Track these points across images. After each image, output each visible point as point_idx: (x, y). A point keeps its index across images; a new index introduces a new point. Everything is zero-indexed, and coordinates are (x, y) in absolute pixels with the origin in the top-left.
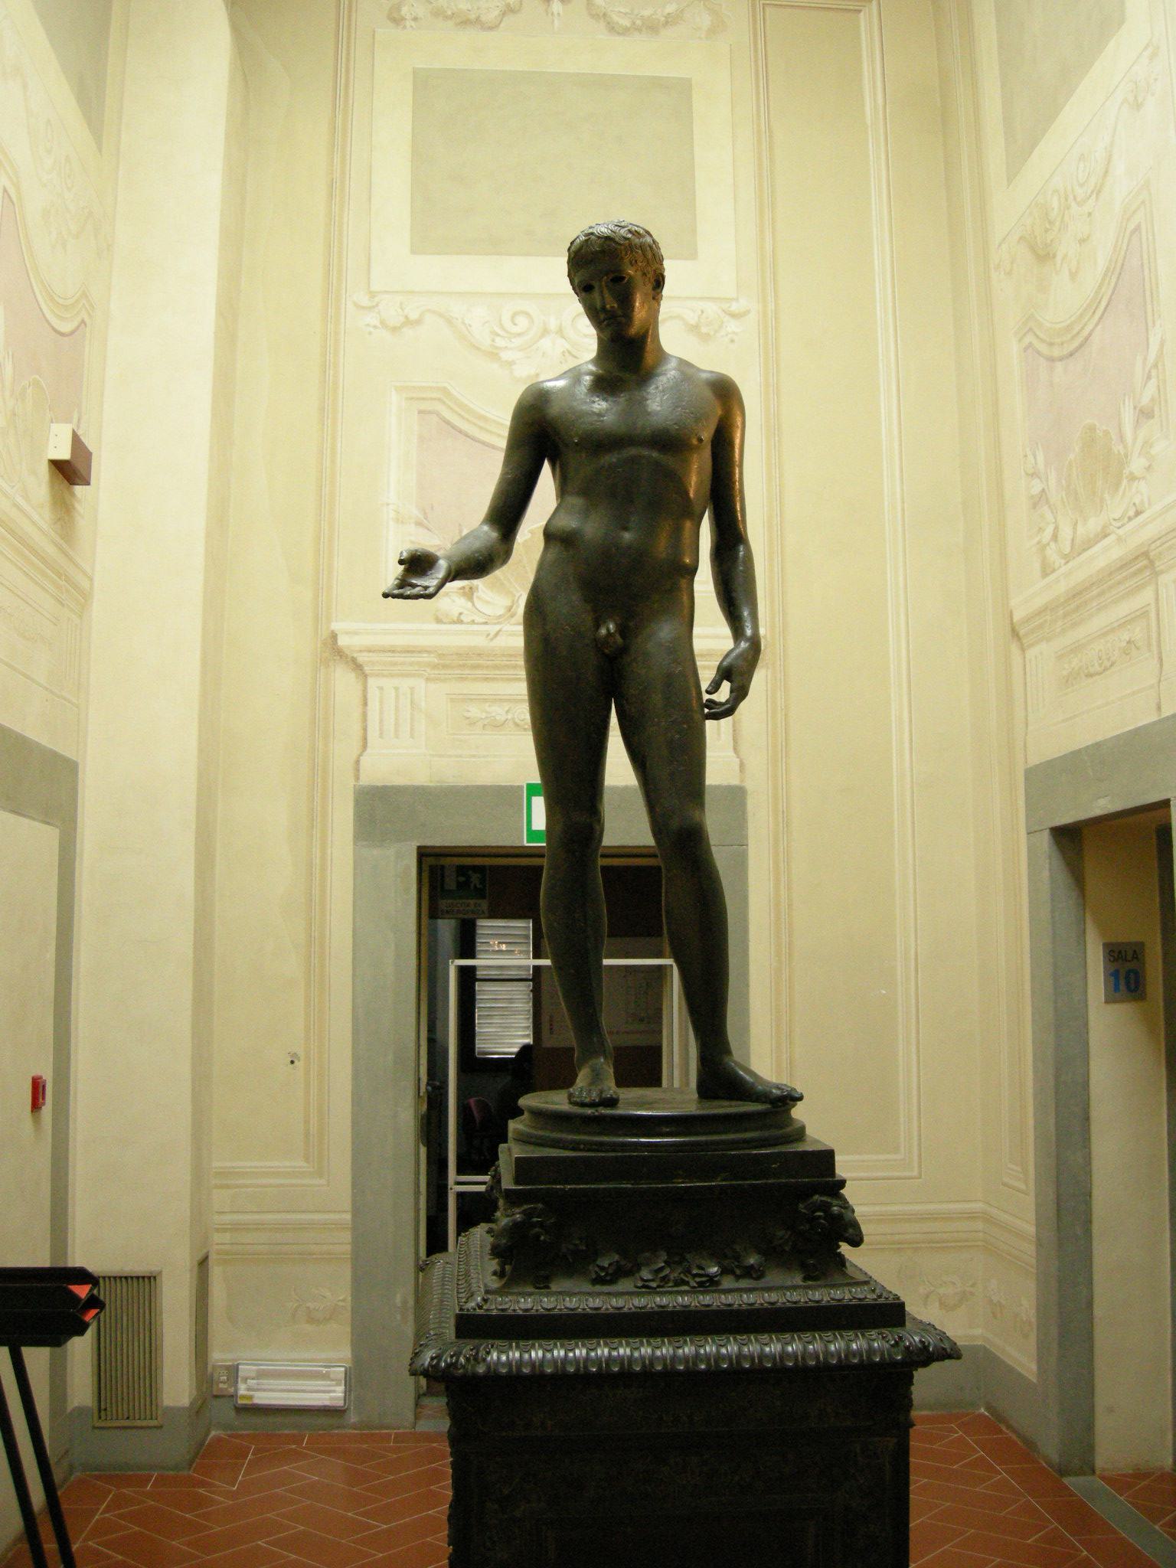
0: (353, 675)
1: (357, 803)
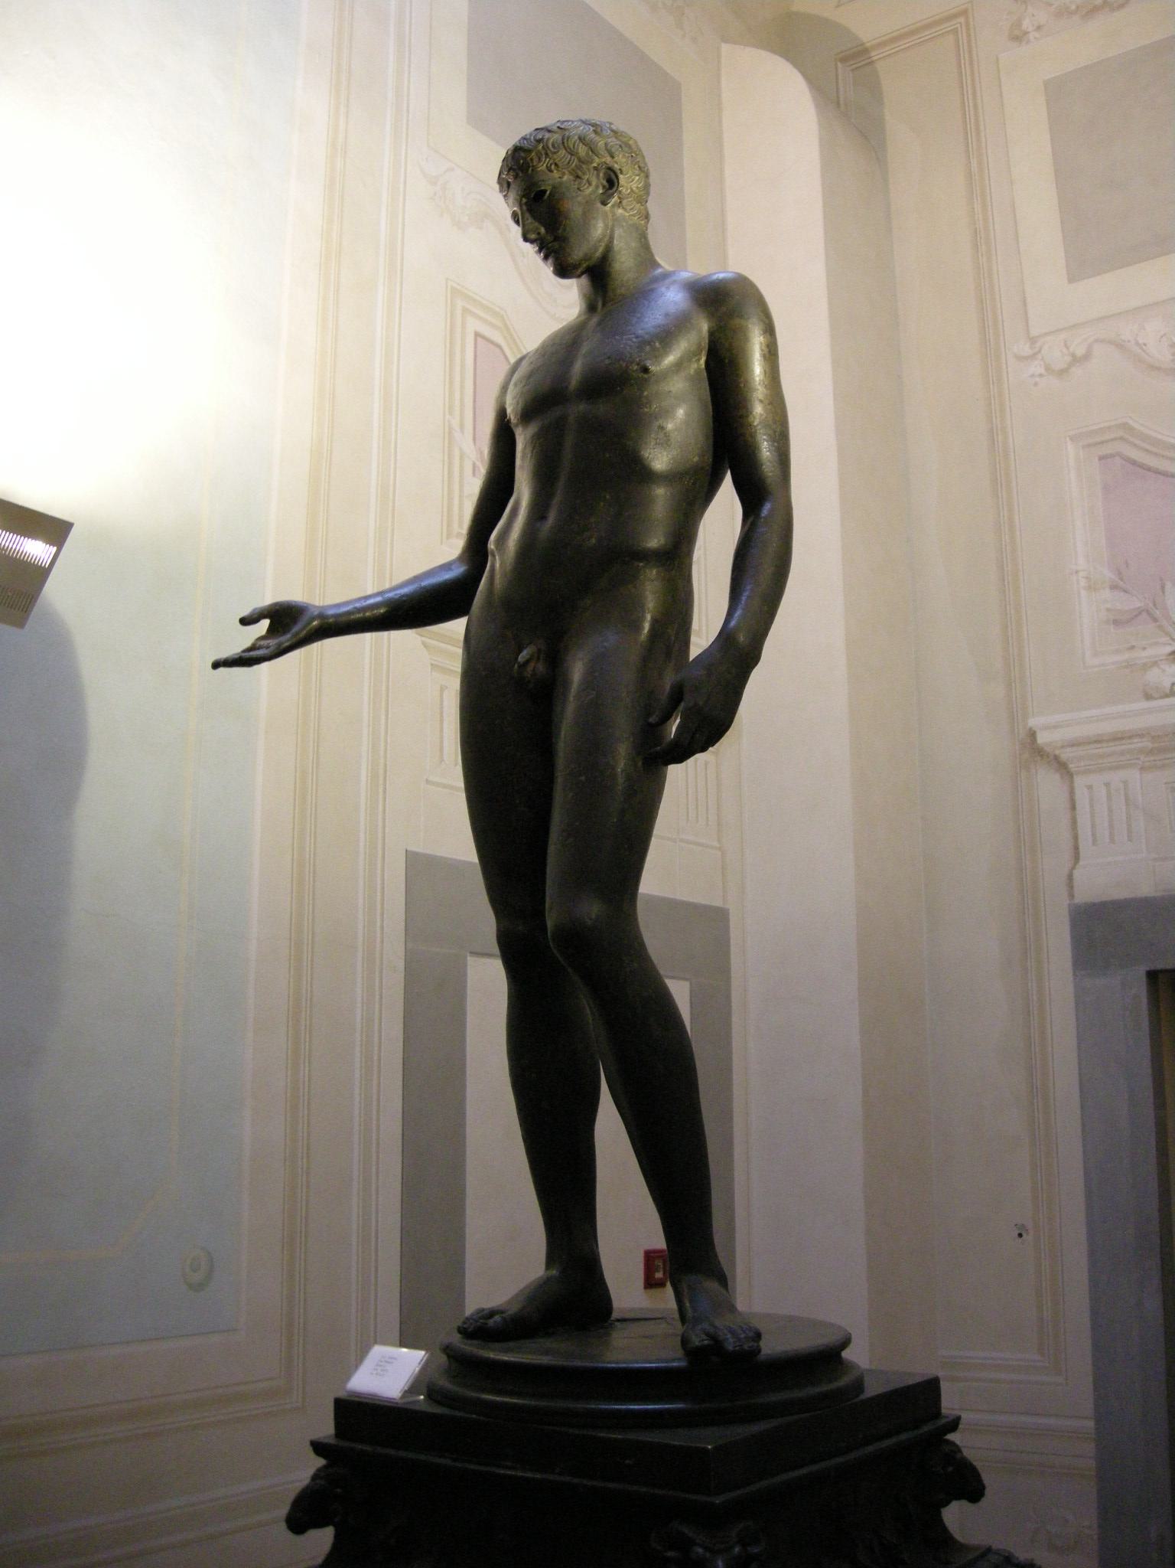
0: (1057, 776)
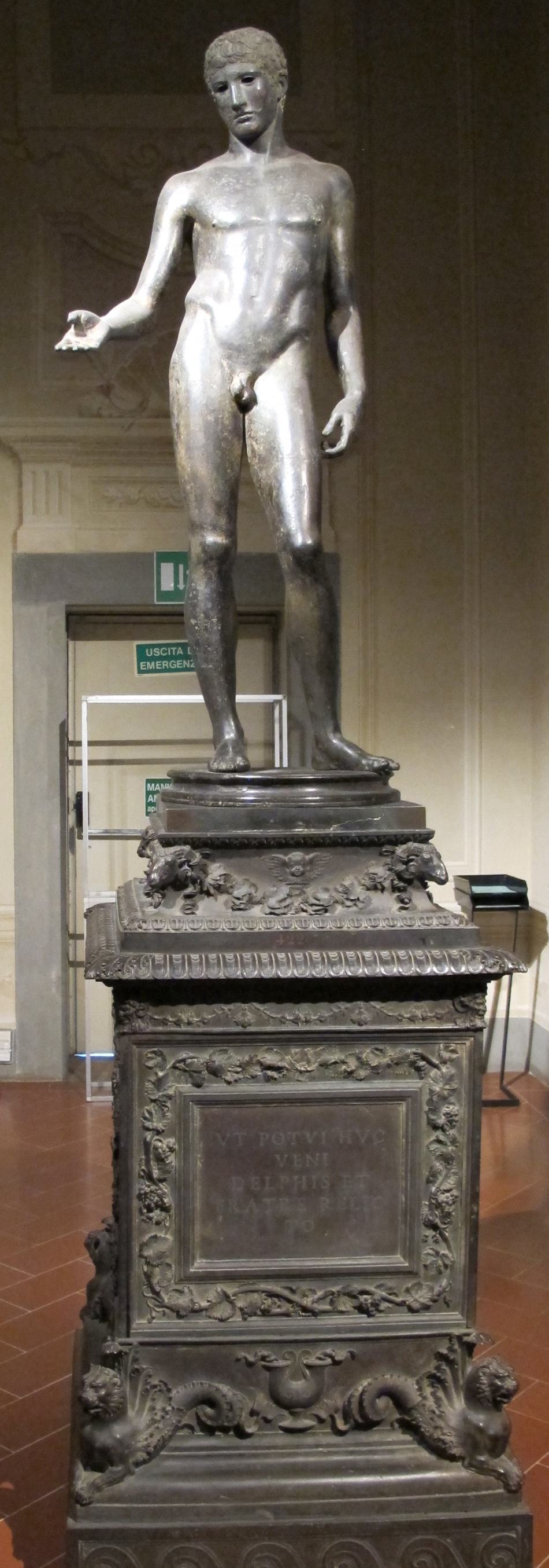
1: (16, 569)
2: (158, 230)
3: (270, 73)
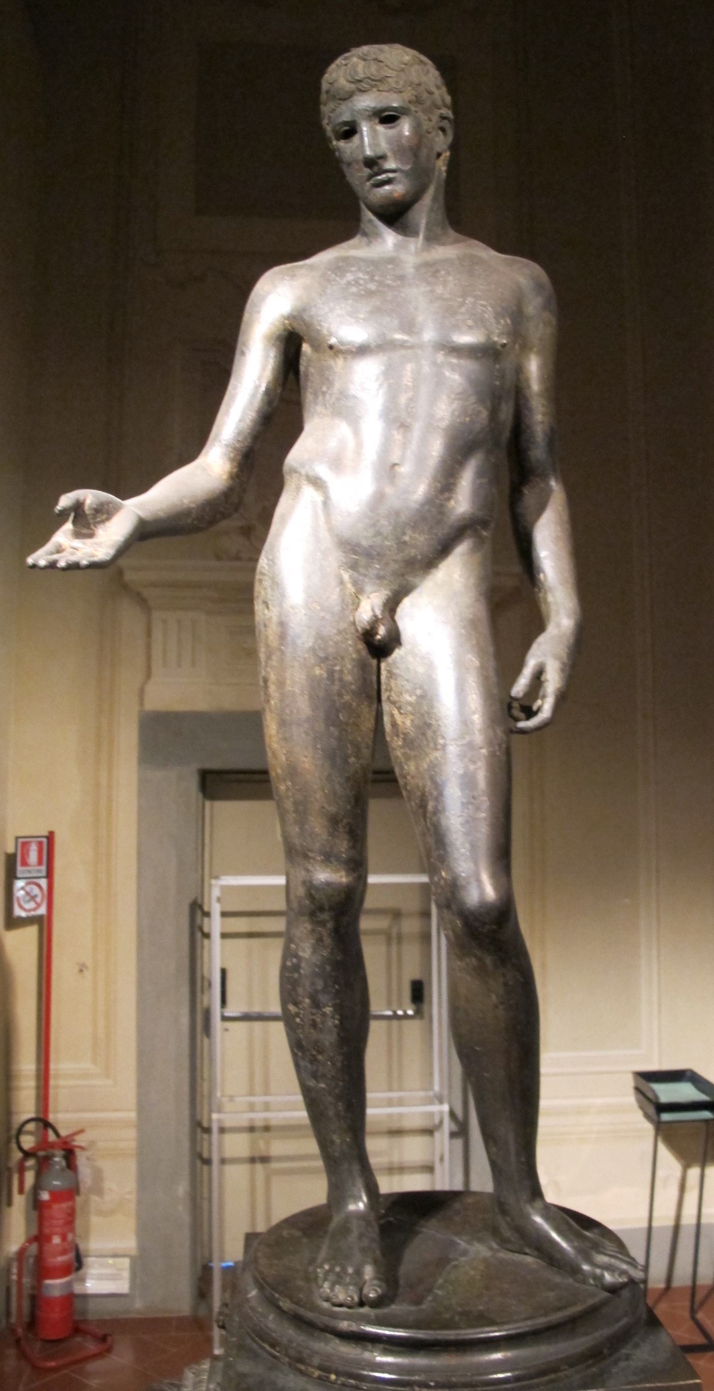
2: (243, 353)
3: (425, 111)
